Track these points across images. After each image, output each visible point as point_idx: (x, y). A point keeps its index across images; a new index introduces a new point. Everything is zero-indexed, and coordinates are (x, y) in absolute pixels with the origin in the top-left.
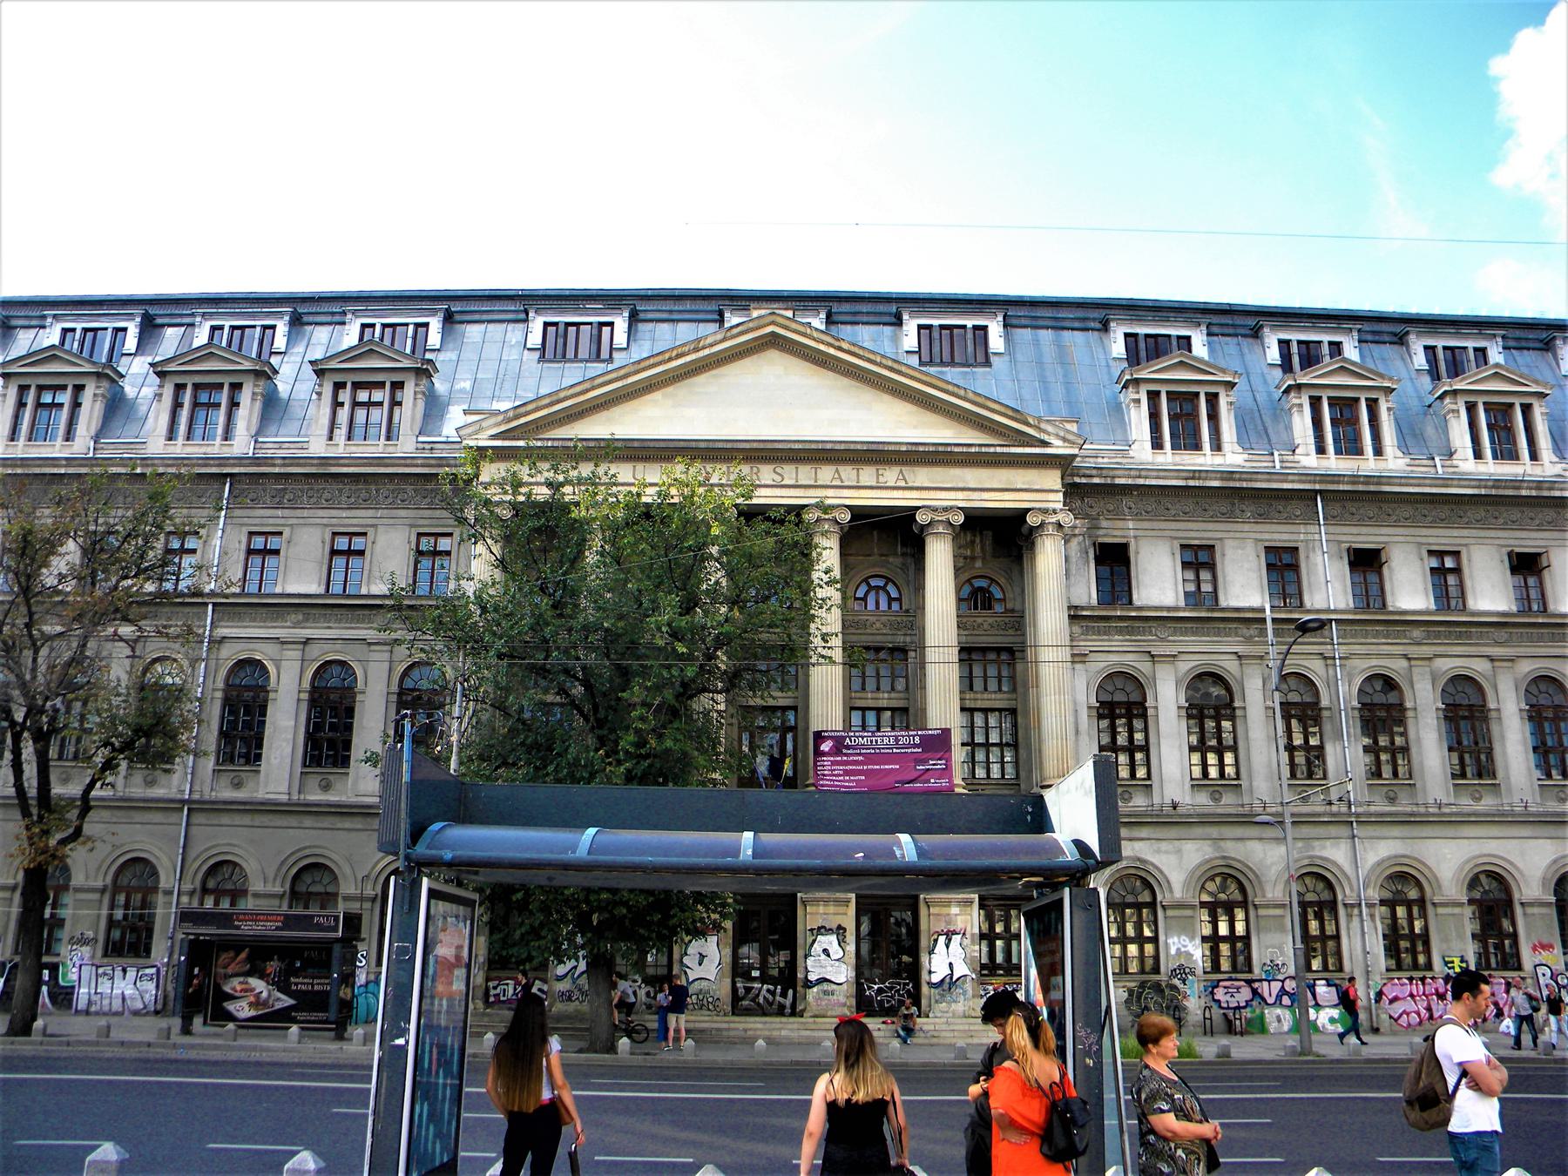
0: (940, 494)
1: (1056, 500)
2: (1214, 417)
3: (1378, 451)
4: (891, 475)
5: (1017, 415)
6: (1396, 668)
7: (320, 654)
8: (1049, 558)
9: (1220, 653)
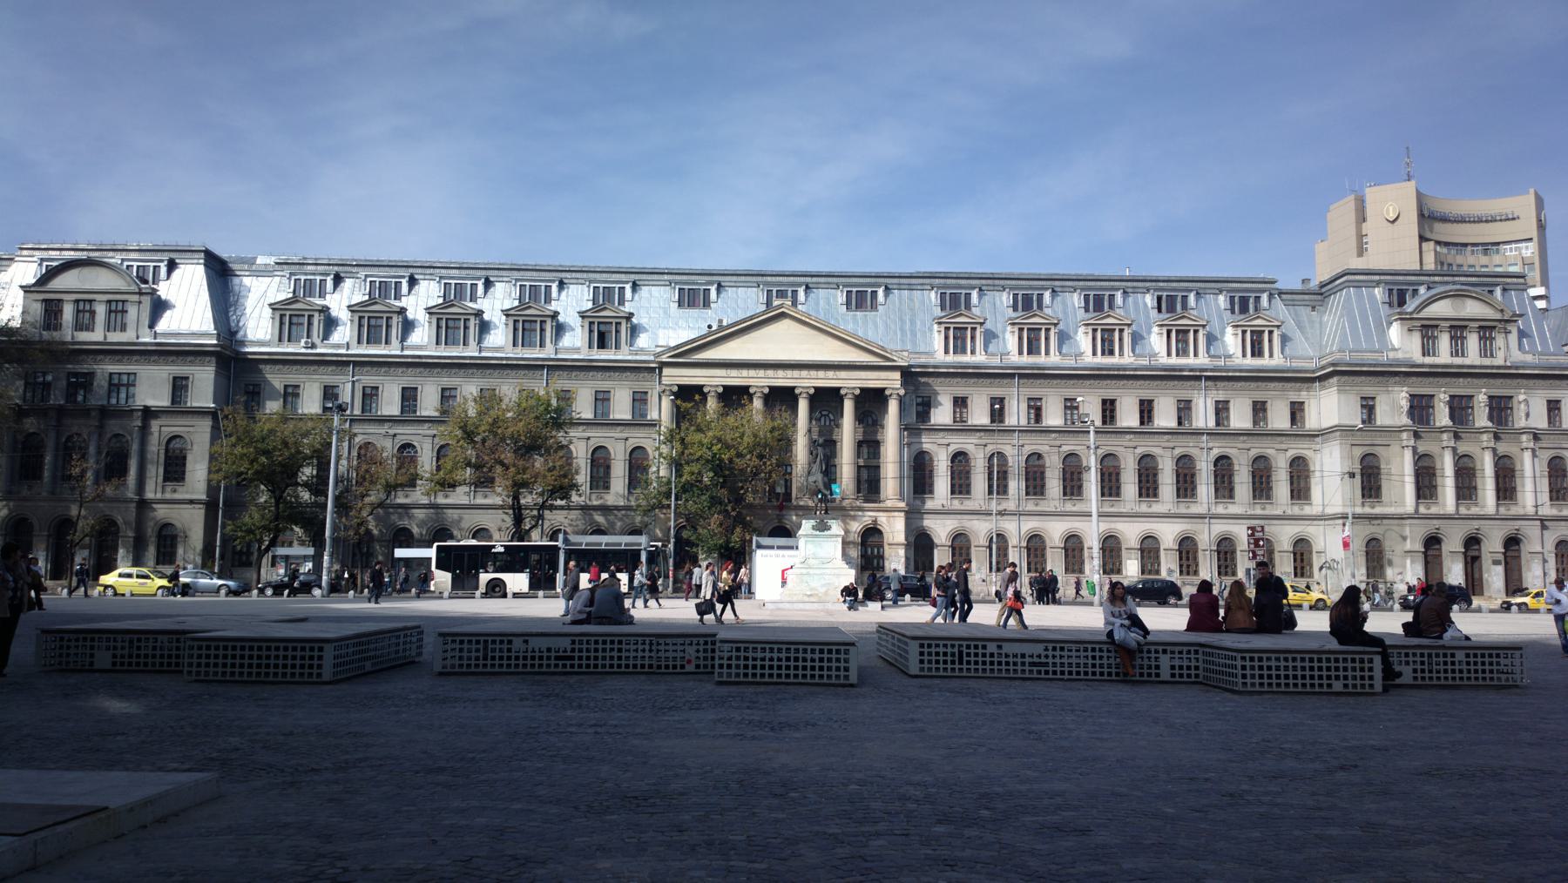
0: (850, 382)
1: (898, 384)
2: (973, 338)
3: (1047, 353)
4: (830, 374)
5: (883, 348)
6: (1043, 449)
7: (593, 443)
8: (893, 406)
9: (968, 443)
